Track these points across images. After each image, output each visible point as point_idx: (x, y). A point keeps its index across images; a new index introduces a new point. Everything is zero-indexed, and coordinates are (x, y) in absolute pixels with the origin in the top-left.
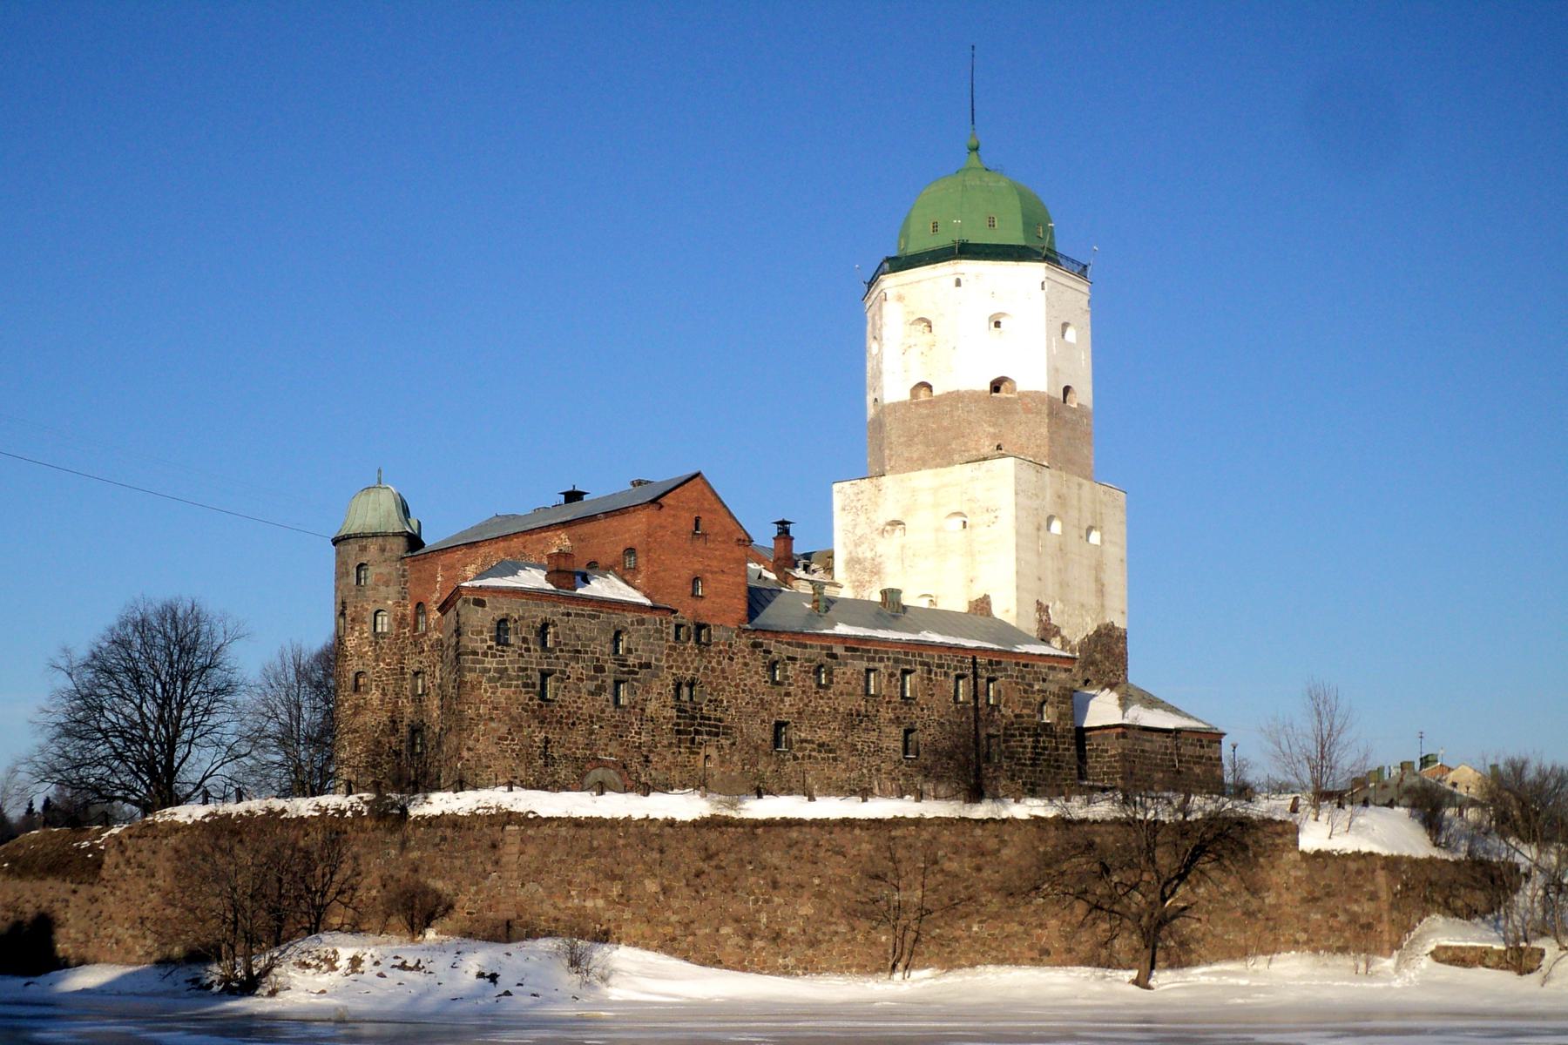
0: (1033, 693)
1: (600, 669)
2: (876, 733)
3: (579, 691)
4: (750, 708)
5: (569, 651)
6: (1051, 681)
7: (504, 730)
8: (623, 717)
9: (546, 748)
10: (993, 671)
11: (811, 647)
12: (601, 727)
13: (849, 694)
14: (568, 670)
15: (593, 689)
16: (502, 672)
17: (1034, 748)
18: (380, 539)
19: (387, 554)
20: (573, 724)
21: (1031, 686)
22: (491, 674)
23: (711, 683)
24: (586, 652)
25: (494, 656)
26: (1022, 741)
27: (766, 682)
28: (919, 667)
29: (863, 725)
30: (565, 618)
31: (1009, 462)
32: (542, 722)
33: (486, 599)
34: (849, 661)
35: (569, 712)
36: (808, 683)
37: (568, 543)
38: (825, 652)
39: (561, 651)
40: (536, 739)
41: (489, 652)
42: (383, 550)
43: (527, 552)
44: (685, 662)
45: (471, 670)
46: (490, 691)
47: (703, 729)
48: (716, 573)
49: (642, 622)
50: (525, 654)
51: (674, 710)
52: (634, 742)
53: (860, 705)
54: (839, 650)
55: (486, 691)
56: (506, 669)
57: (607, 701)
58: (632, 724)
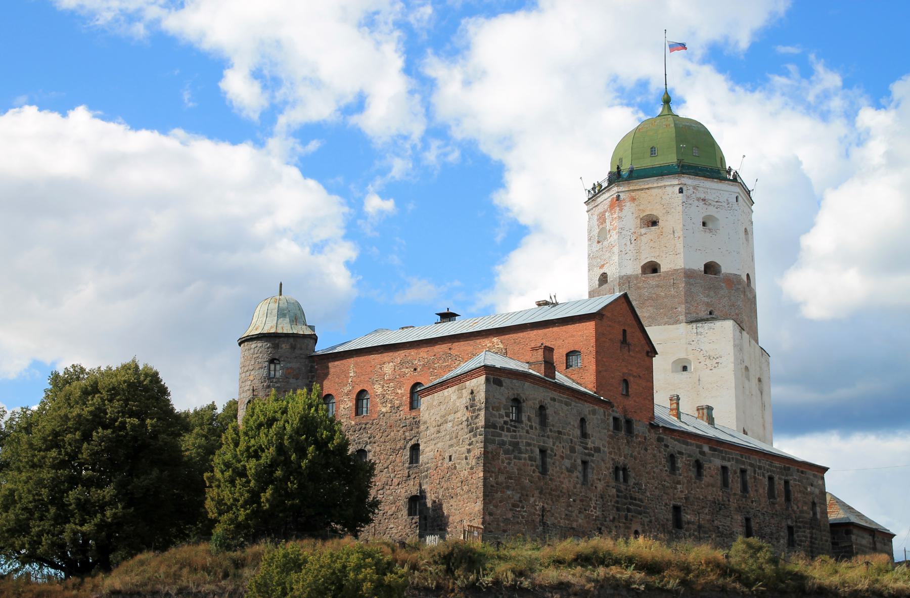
0: (807, 494)
1: (573, 450)
2: (730, 519)
3: (561, 468)
4: (657, 492)
5: (555, 432)
6: (815, 487)
7: (517, 497)
8: (586, 493)
9: (543, 516)
10: (787, 475)
11: (691, 445)
12: (574, 501)
13: (713, 486)
14: (555, 448)
15: (569, 466)
16: (516, 445)
17: (811, 538)
18: (291, 340)
19: (298, 352)
20: (559, 496)
21: (807, 490)
22: (507, 446)
23: (634, 469)
24: (565, 435)
25: (508, 430)
26: (804, 532)
27: (666, 471)
28: (749, 467)
29: (721, 512)
30: (552, 403)
31: (729, 324)
32: (541, 493)
33: (502, 379)
34: (712, 458)
35: (556, 486)
36: (690, 474)
37: (501, 346)
38: (698, 450)
39: (551, 431)
40: (537, 508)
41: (505, 426)
42: (293, 348)
43: (452, 352)
44: (619, 449)
45: (493, 442)
46: (507, 461)
47: (632, 507)
48: (636, 377)
49: (594, 412)
50: (530, 431)
51: (614, 490)
52: (593, 515)
53: (719, 496)
54: (706, 449)
55: (503, 462)
56: (518, 443)
57: (578, 478)
58: (591, 499)
